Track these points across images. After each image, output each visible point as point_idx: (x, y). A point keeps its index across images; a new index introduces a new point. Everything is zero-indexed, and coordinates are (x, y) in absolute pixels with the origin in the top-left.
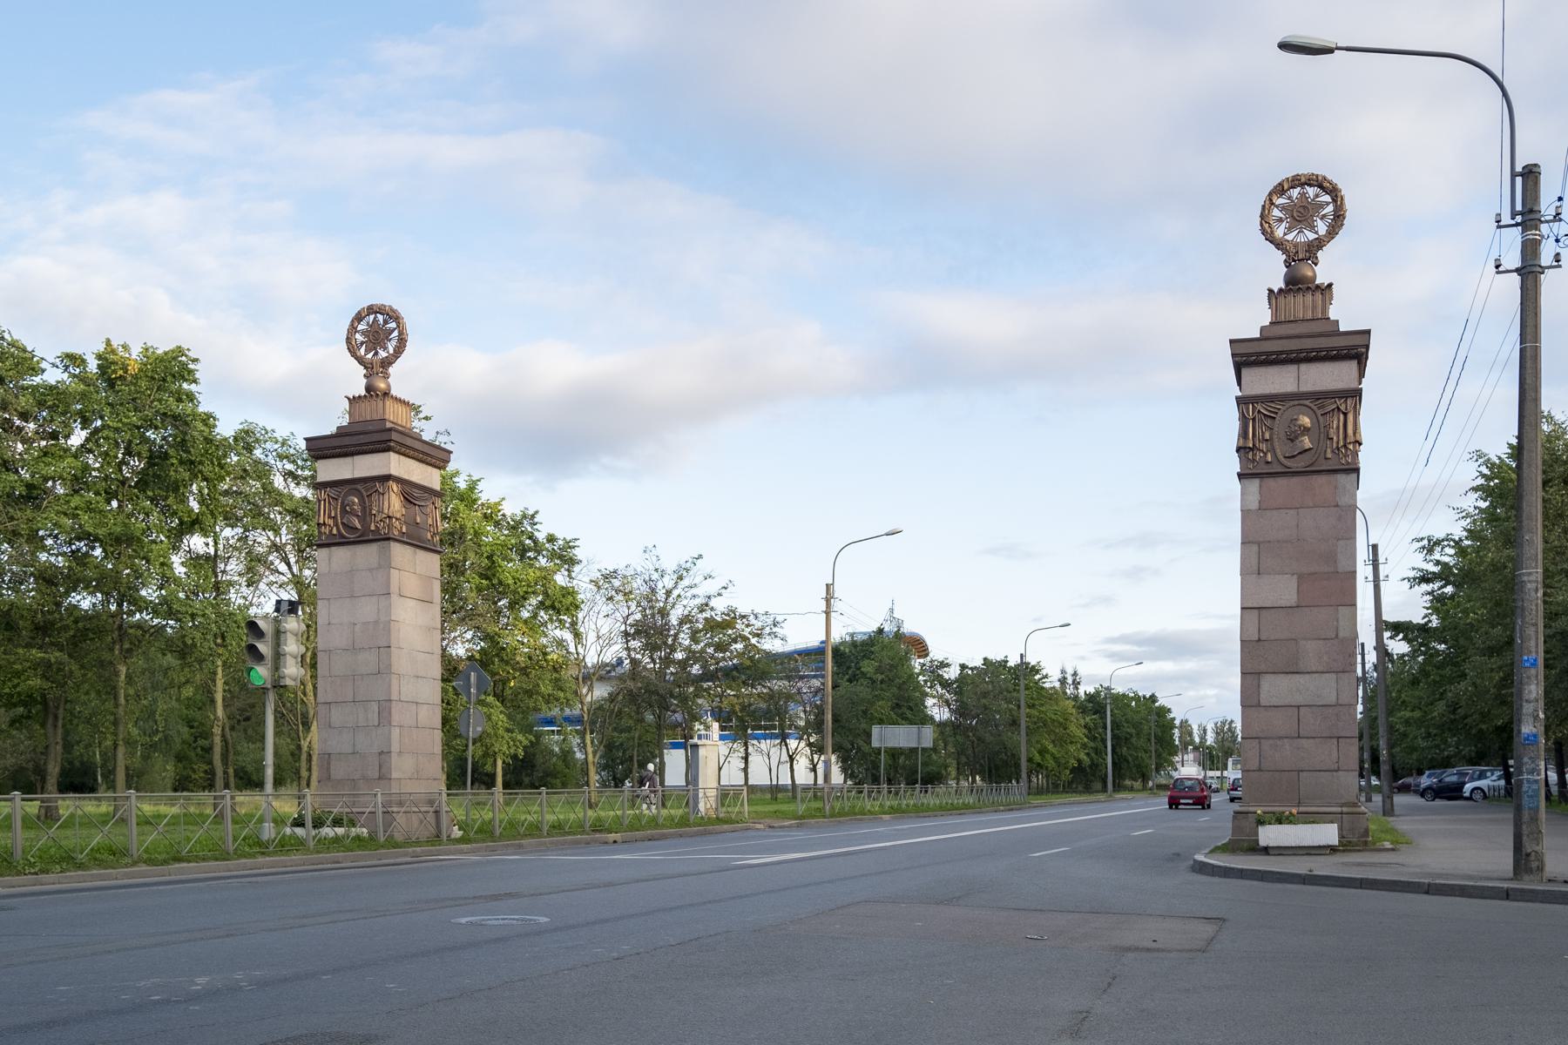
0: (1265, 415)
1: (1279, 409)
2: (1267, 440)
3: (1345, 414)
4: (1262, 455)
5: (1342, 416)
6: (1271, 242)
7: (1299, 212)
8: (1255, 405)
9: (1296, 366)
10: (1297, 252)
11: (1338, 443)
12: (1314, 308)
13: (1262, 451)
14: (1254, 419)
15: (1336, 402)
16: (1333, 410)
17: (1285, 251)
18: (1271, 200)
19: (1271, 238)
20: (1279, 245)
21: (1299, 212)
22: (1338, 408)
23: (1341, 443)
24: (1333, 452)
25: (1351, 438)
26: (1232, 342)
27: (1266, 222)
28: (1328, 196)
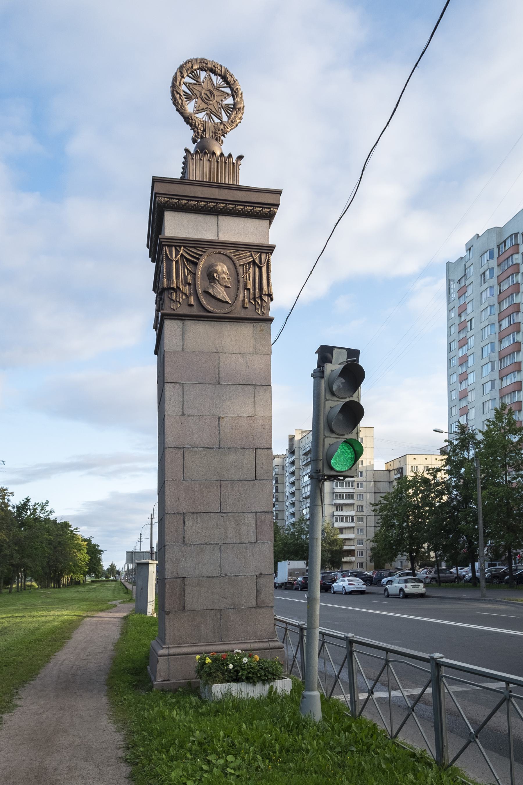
0: (187, 260)
1: (201, 255)
2: (189, 284)
3: (260, 268)
4: (184, 297)
5: (257, 270)
6: (182, 114)
7: (206, 94)
8: (178, 248)
9: (216, 217)
10: (204, 130)
11: (254, 294)
12: (227, 173)
13: (186, 295)
14: (177, 262)
15: (251, 256)
16: (249, 263)
17: (193, 127)
18: (181, 73)
19: (181, 111)
20: (187, 119)
21: (206, 94)
22: (254, 261)
23: (257, 295)
24: (250, 302)
25: (265, 291)
26: (153, 177)
27: (178, 93)
28: (229, 89)
